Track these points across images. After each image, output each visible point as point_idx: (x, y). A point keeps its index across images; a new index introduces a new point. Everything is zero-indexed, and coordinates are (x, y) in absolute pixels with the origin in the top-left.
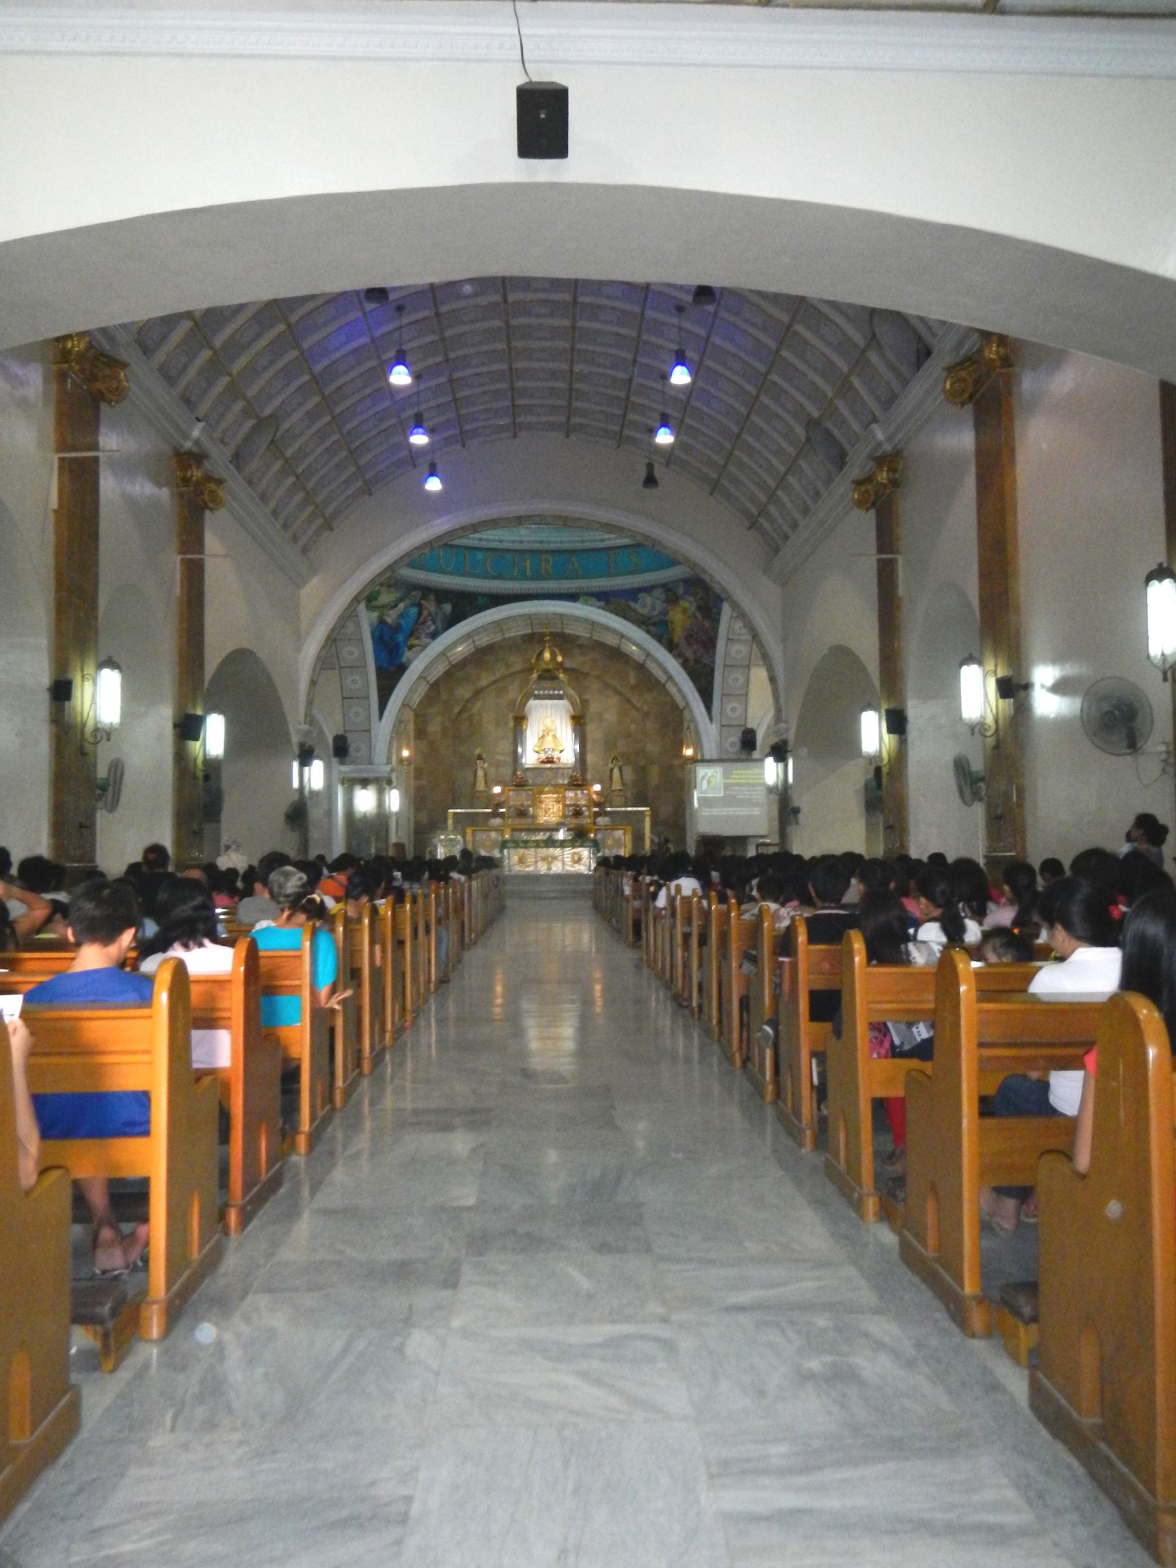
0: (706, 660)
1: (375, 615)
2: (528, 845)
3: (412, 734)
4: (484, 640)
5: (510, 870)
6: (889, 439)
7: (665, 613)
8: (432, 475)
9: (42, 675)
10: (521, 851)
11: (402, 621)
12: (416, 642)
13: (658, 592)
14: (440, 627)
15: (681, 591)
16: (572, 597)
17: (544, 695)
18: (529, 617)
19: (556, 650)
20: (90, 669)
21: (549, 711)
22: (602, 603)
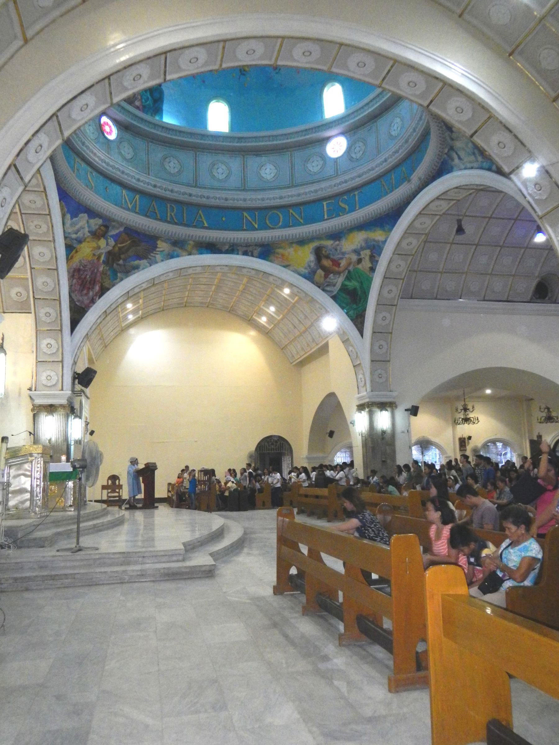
15: (113, 232)
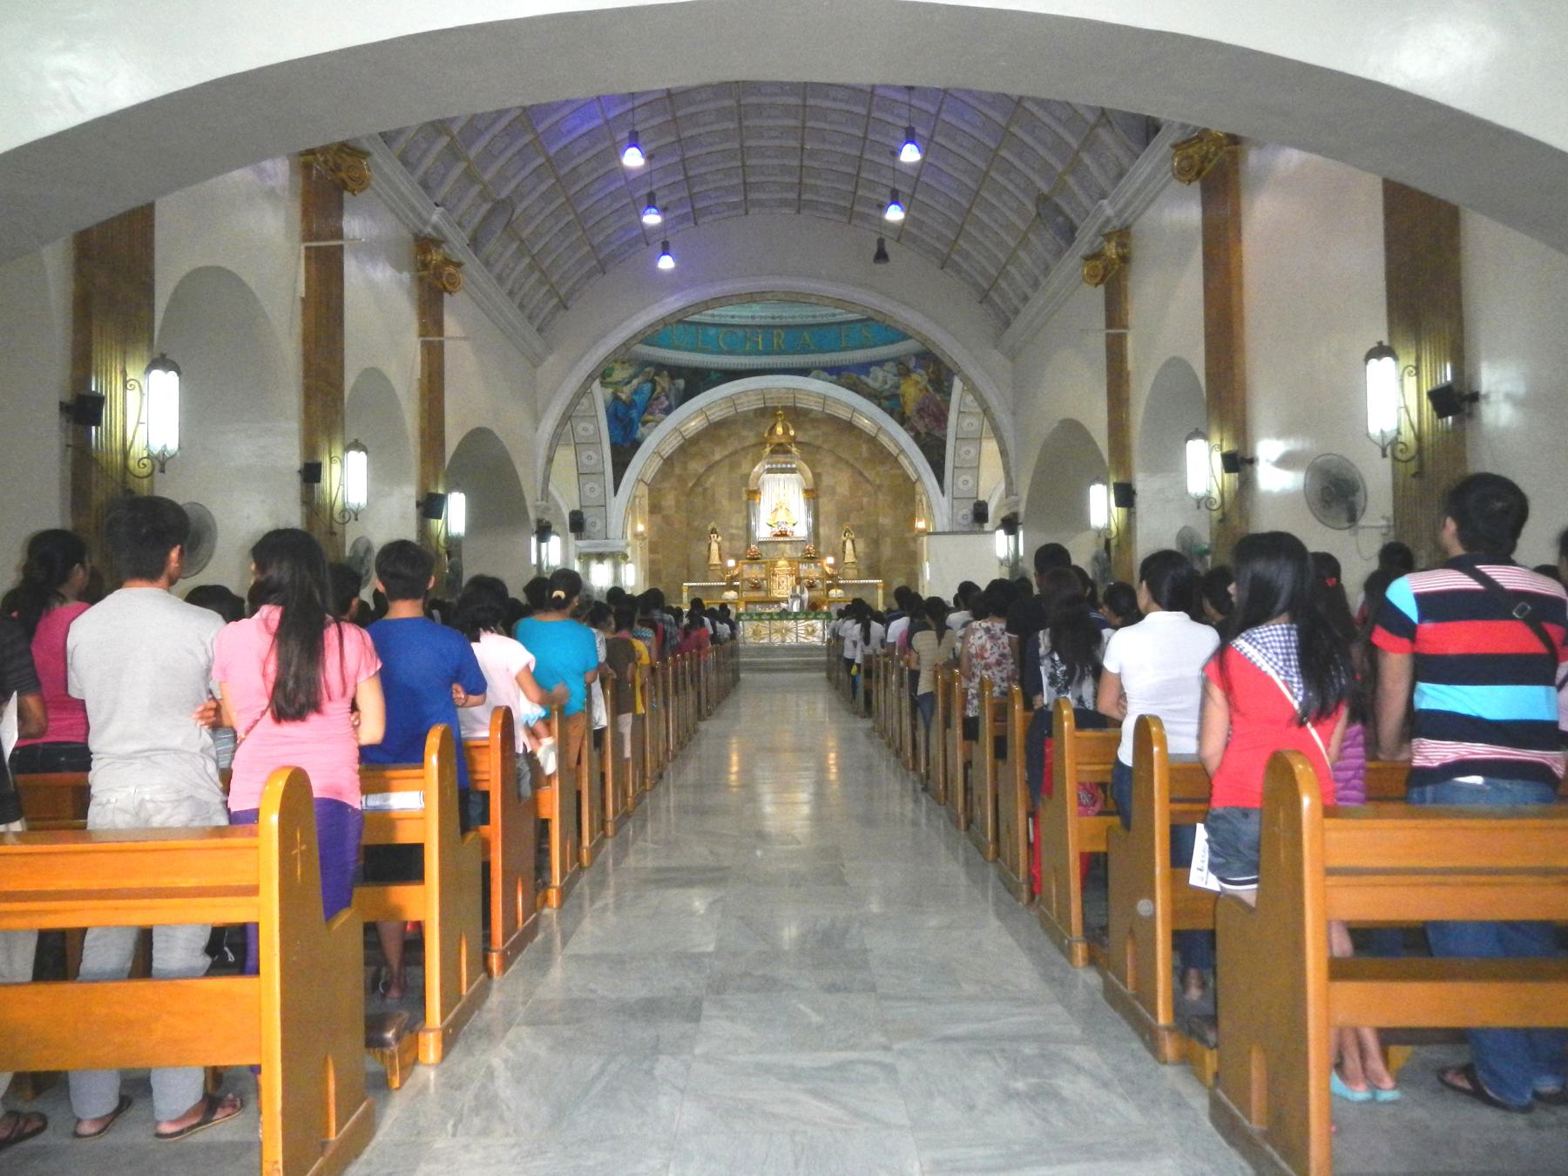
0: (937, 433)
1: (610, 391)
2: (763, 617)
3: (647, 509)
4: (716, 415)
5: (745, 643)
6: (1119, 214)
7: (897, 387)
8: (665, 253)
9: (294, 460)
10: (756, 623)
11: (636, 398)
12: (650, 417)
13: (889, 366)
14: (673, 403)
16: (803, 372)
17: (777, 469)
18: (762, 392)
19: (790, 425)
20: (337, 451)
21: (782, 484)
22: (834, 377)
